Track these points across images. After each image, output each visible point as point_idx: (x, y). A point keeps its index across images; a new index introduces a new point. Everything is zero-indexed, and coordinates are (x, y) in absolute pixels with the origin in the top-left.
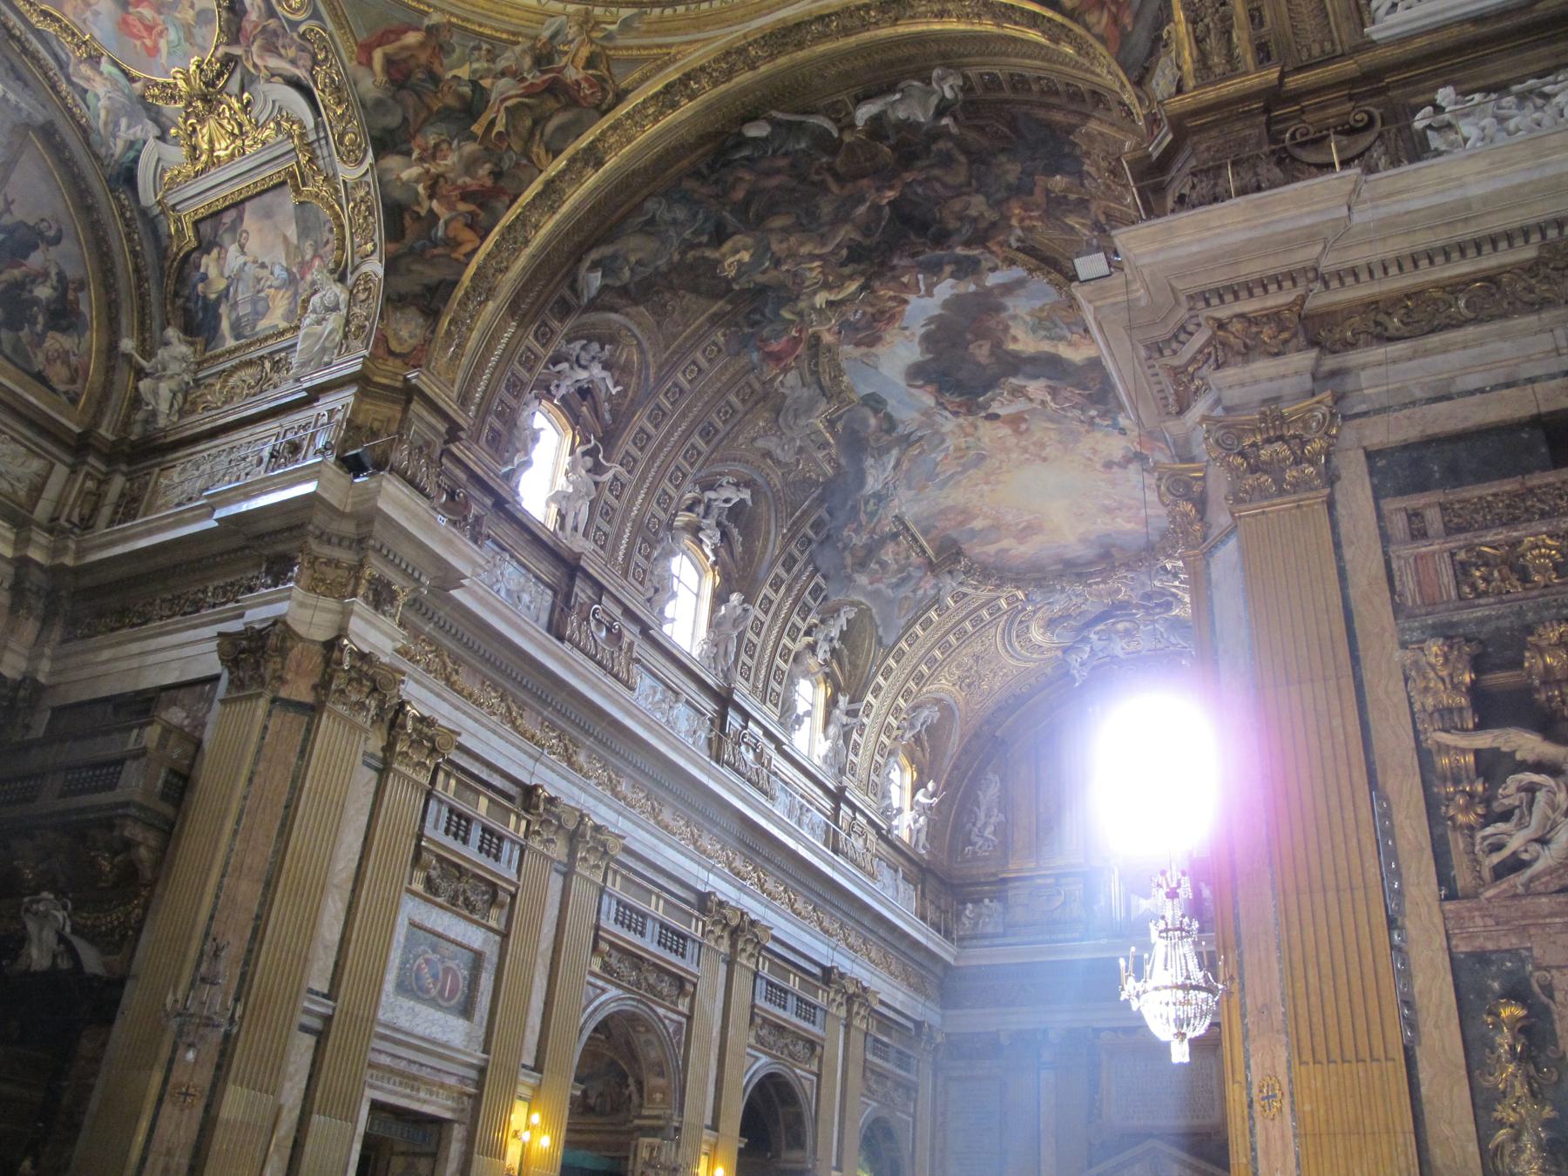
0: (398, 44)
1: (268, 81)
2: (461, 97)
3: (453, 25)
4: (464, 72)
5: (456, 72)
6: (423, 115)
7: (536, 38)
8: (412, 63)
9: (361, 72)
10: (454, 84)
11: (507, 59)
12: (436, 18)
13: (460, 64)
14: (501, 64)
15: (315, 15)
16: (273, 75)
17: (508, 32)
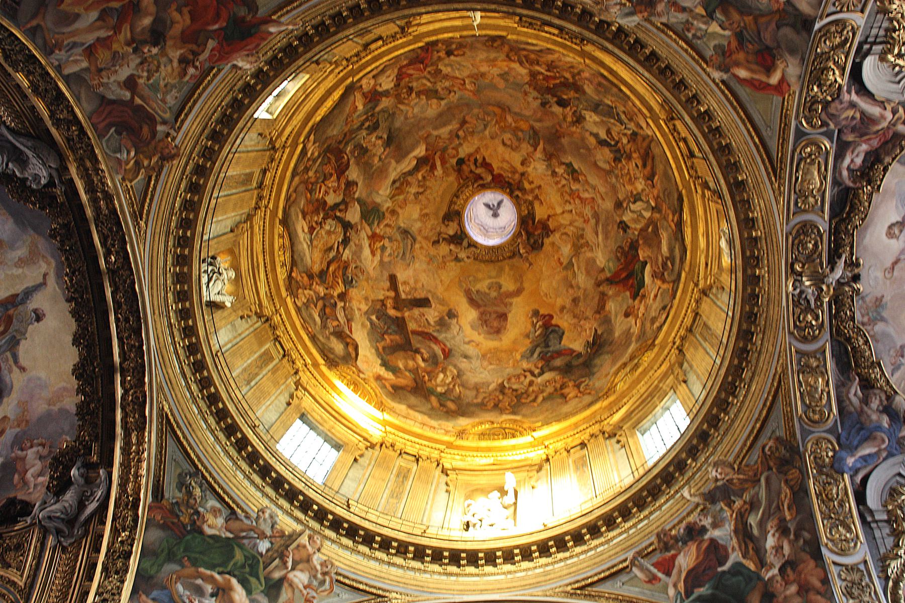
0: (756, 77)
1: (889, 101)
2: (725, 13)
3: (706, 63)
4: (714, 28)
5: (722, 32)
6: (763, 20)
7: (647, 20)
8: (751, 58)
9: (792, 80)
10: (727, 24)
11: (676, 17)
12: (717, 75)
13: (714, 35)
14: (682, 17)
15: (800, 134)
16: (882, 102)
17: (666, 34)
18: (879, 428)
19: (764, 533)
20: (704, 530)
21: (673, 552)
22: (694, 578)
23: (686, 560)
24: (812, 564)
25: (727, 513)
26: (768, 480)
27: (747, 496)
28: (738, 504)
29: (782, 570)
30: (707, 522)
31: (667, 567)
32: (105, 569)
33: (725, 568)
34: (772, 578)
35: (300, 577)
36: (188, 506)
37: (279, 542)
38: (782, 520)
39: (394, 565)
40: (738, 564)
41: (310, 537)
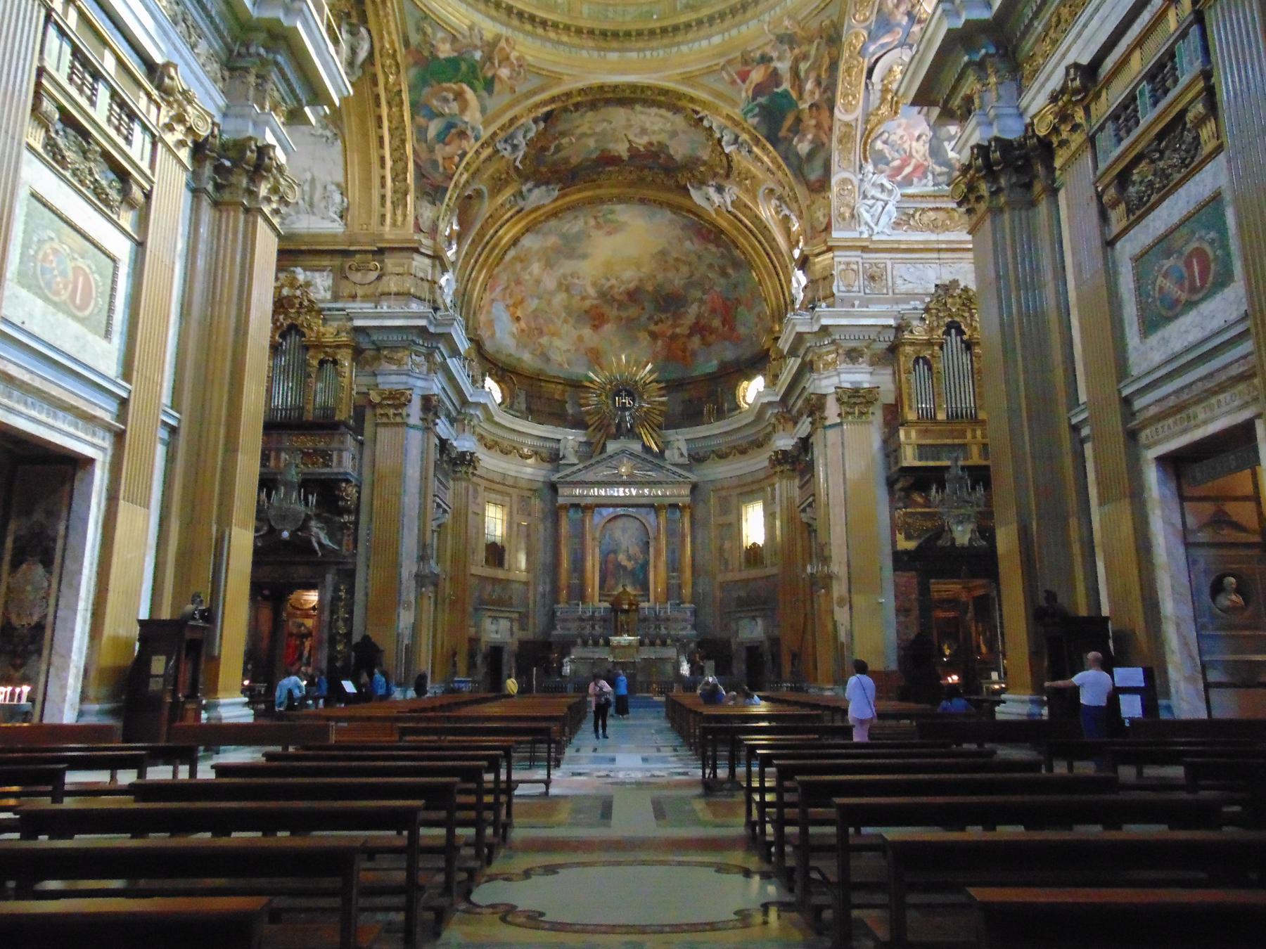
18: (899, 25)
19: (807, 79)
20: (771, 59)
21: (747, 68)
22: (759, 90)
23: (757, 75)
24: (827, 114)
25: (788, 54)
26: (819, 44)
27: (804, 48)
28: (797, 51)
29: (811, 106)
30: (775, 54)
31: (744, 77)
32: (389, 104)
33: (779, 90)
34: (803, 110)
35: (504, 72)
36: (426, 42)
37: (486, 49)
38: (819, 76)
39: (559, 43)
40: (786, 91)
41: (507, 40)
